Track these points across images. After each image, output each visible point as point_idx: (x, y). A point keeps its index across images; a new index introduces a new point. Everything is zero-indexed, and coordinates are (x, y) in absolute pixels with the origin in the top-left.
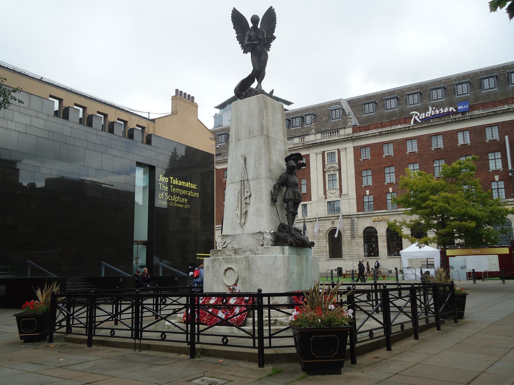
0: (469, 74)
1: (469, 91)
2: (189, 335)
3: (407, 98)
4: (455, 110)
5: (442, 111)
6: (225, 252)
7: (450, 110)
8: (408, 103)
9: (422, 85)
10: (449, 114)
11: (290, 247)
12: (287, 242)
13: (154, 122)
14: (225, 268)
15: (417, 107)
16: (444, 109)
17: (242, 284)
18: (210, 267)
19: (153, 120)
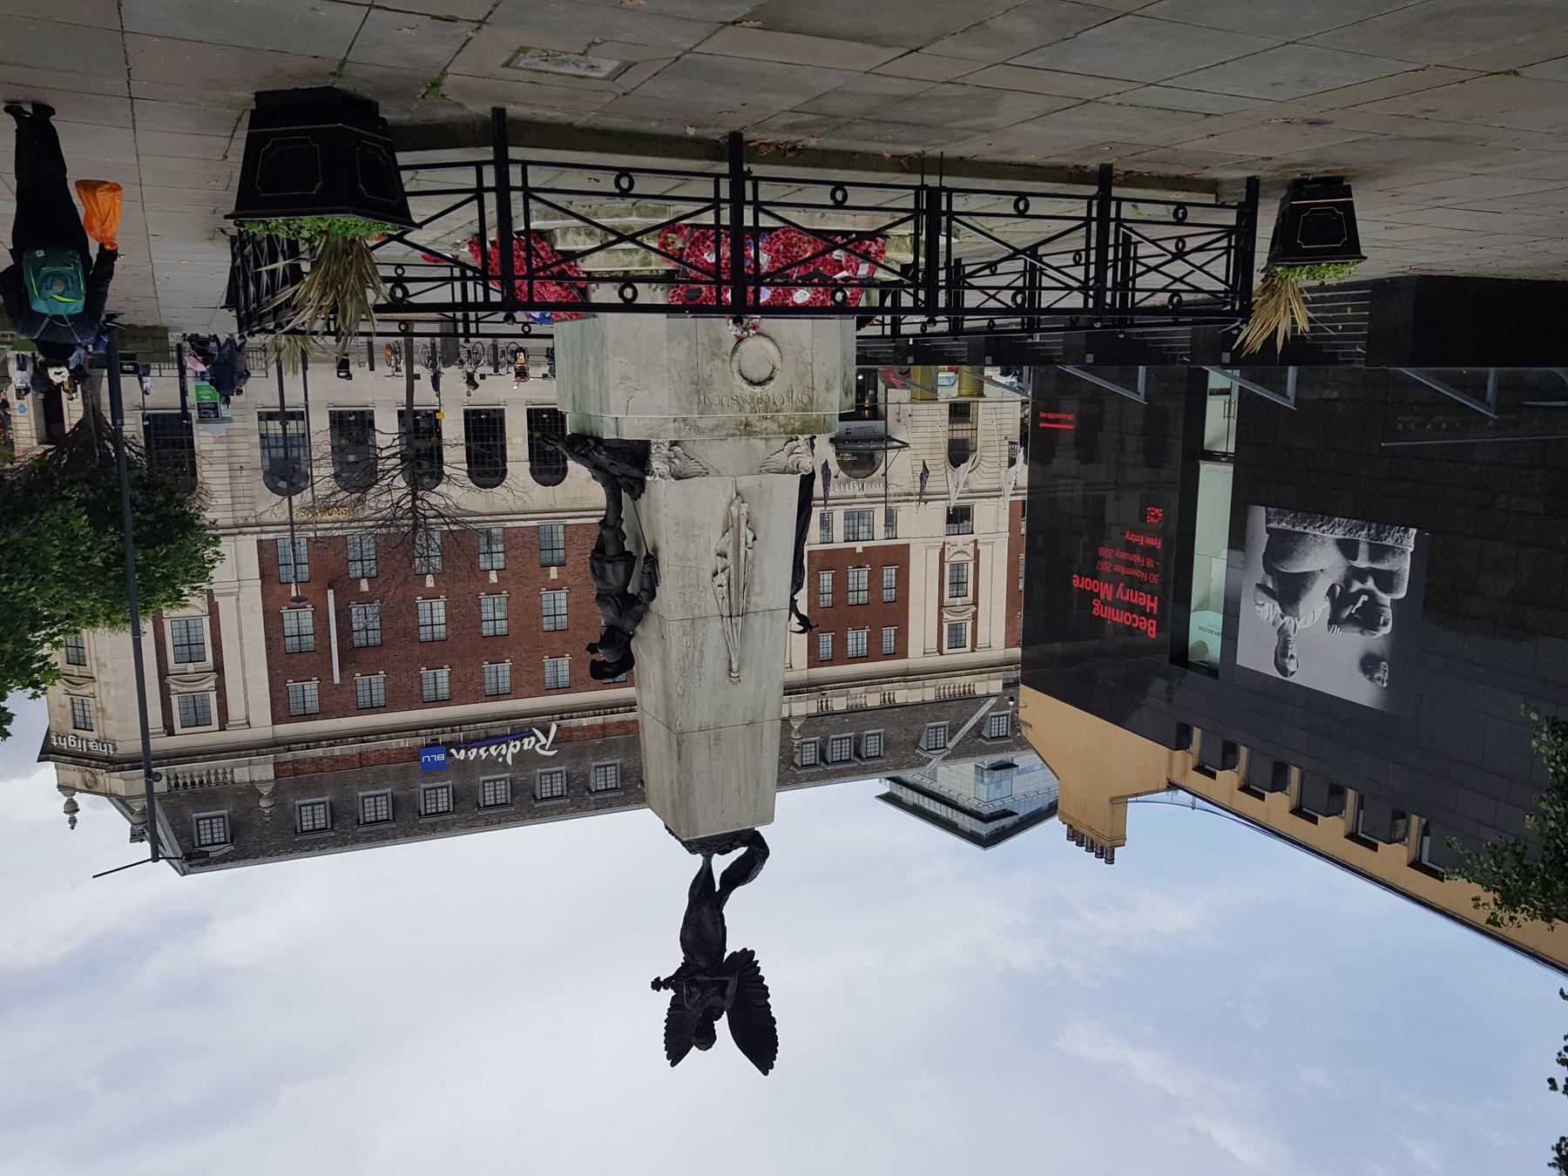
0: (422, 833)
1: (422, 794)
2: (944, 208)
3: (565, 789)
4: (453, 751)
5: (482, 751)
6: (779, 427)
7: (463, 752)
8: (565, 777)
9: (530, 818)
10: (468, 744)
12: (607, 449)
13: (1170, 783)
14: (772, 384)
15: (544, 764)
16: (478, 756)
17: (719, 342)
18: (820, 385)
19: (1172, 786)
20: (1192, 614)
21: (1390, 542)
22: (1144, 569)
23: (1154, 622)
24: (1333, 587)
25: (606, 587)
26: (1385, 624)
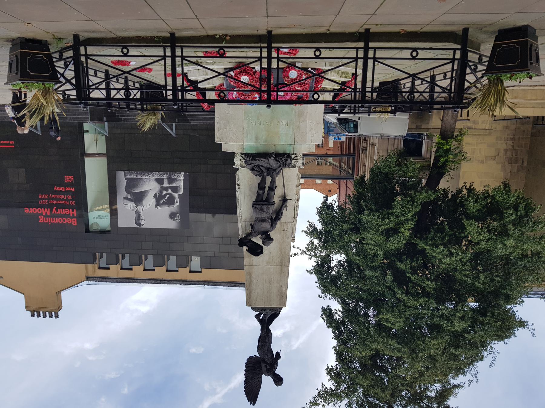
11: (289, 153)
13: (87, 277)
19: (88, 278)
20: (89, 213)
21: (175, 177)
22: (67, 200)
23: (75, 219)
24: (156, 195)
25: (268, 215)
26: (177, 202)
